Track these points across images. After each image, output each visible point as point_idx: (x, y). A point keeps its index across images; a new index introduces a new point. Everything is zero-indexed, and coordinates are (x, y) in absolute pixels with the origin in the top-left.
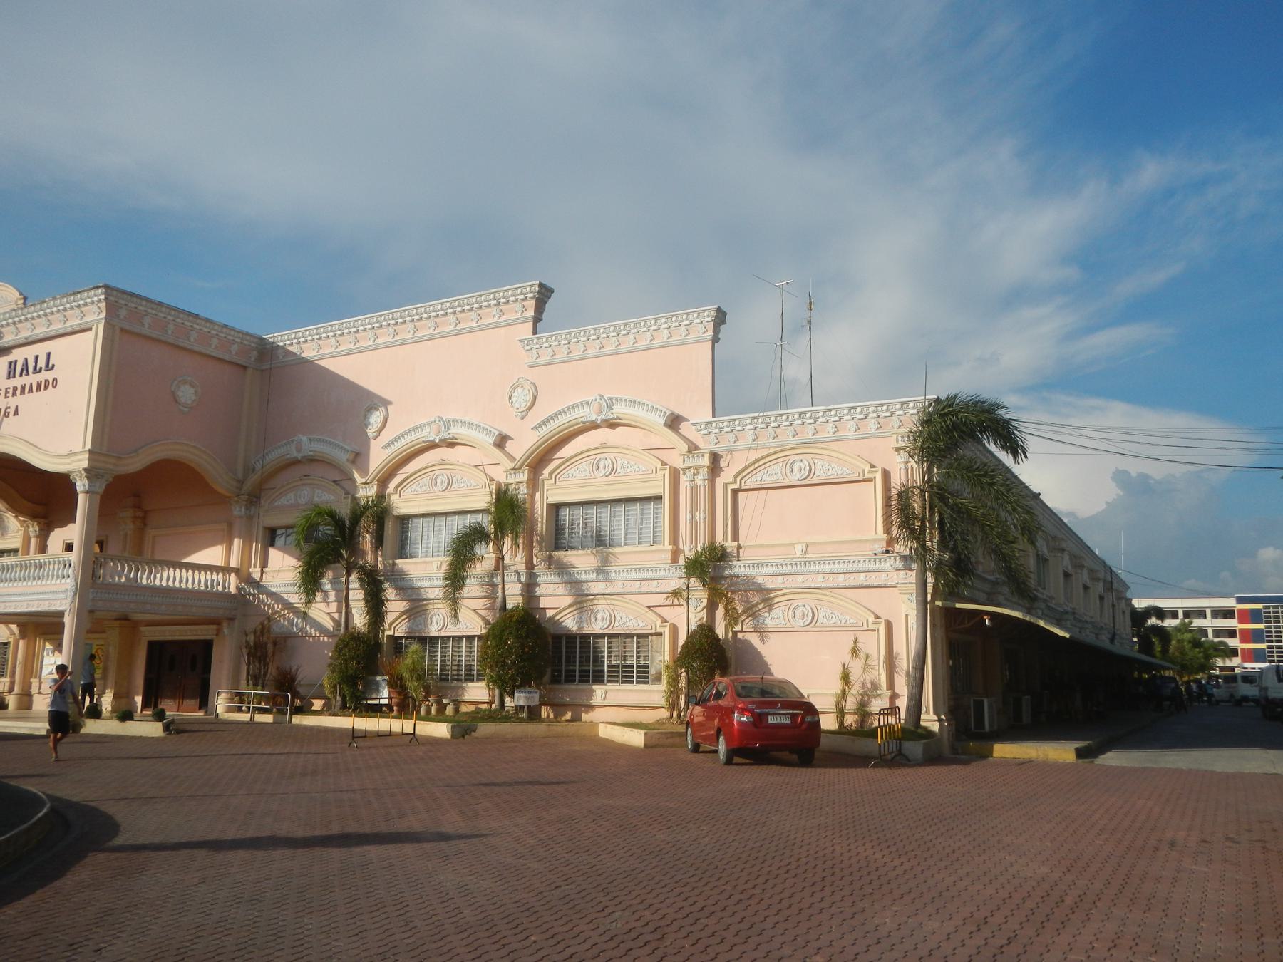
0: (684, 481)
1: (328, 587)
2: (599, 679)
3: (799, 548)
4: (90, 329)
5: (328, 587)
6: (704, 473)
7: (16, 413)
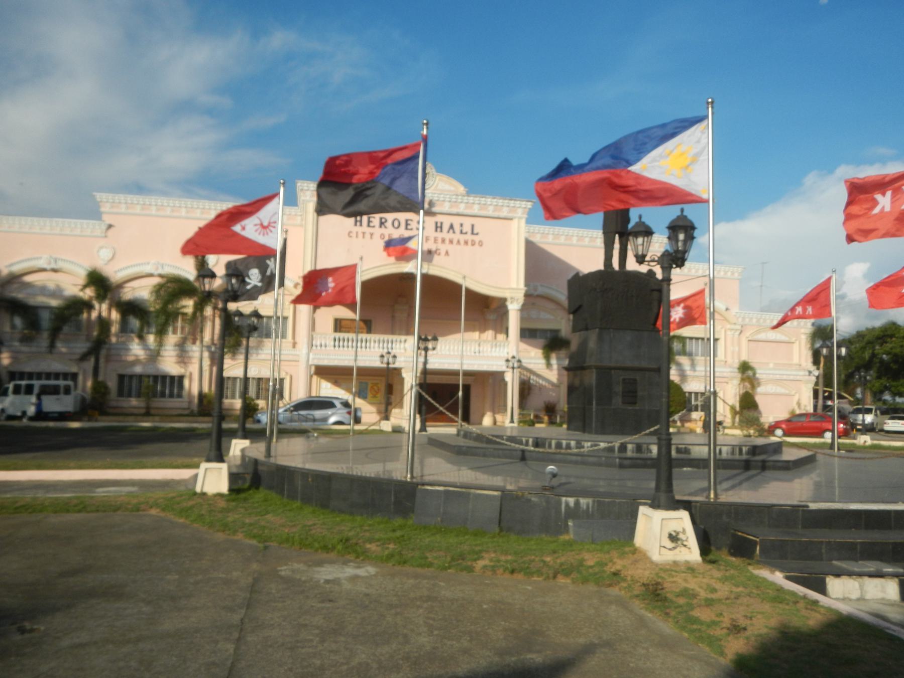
0: (729, 333)
1: (554, 361)
2: (690, 410)
3: (771, 365)
4: (511, 219)
5: (554, 361)
6: (738, 332)
7: (447, 253)
